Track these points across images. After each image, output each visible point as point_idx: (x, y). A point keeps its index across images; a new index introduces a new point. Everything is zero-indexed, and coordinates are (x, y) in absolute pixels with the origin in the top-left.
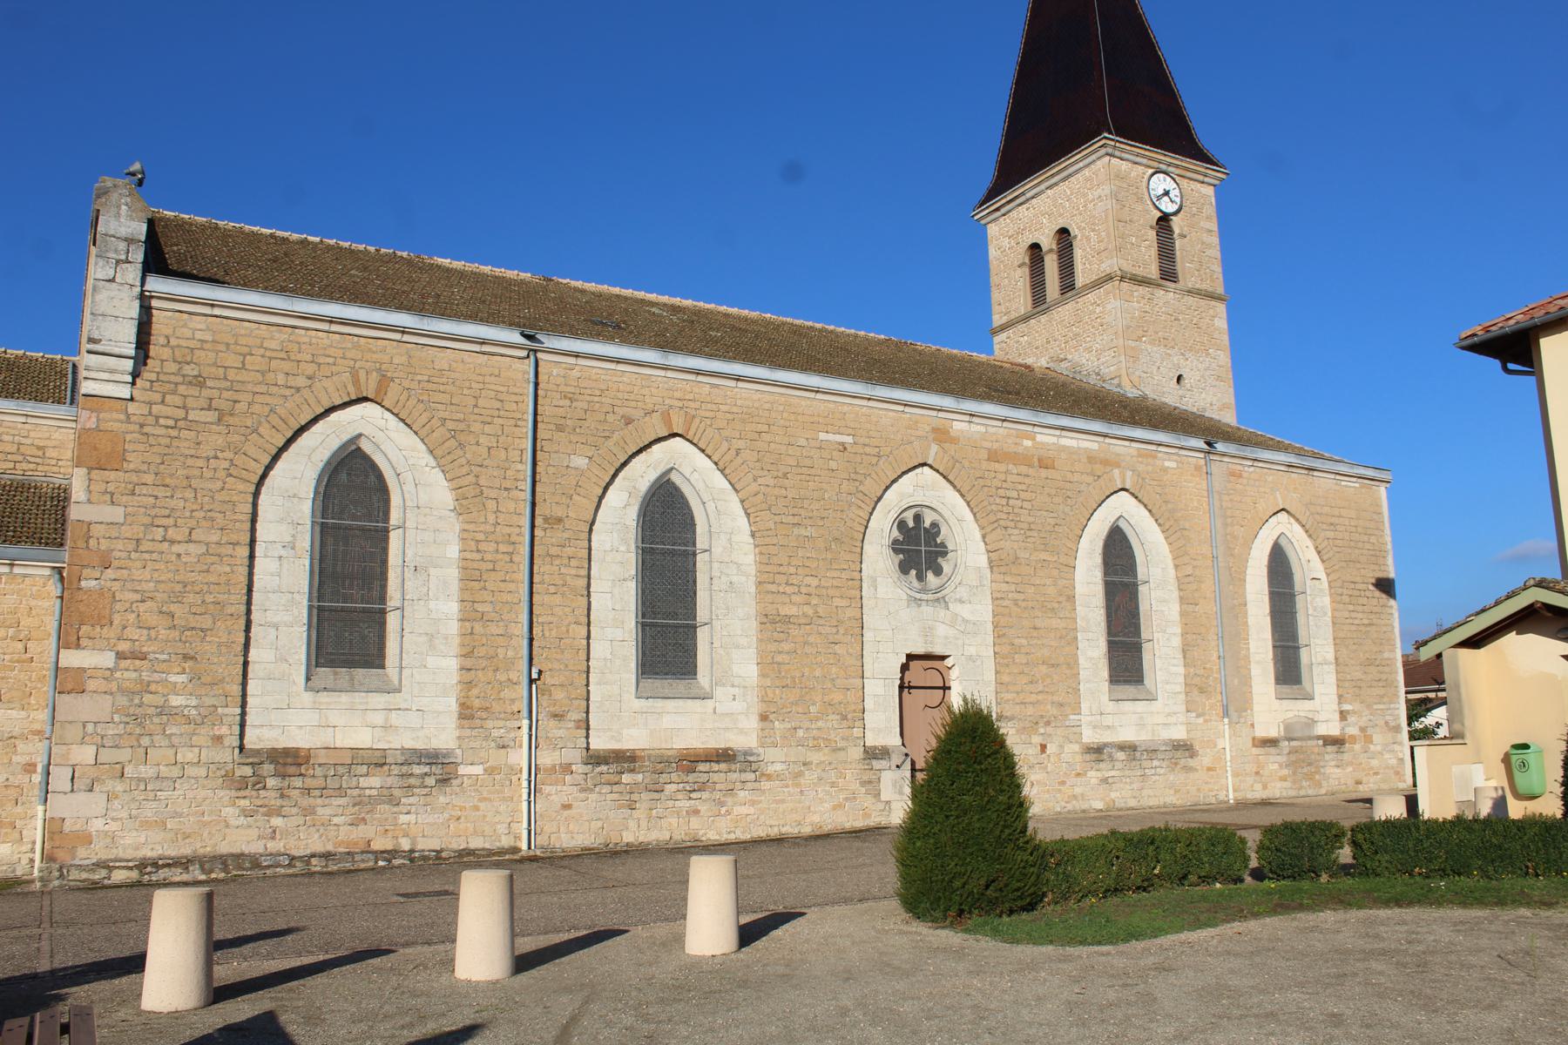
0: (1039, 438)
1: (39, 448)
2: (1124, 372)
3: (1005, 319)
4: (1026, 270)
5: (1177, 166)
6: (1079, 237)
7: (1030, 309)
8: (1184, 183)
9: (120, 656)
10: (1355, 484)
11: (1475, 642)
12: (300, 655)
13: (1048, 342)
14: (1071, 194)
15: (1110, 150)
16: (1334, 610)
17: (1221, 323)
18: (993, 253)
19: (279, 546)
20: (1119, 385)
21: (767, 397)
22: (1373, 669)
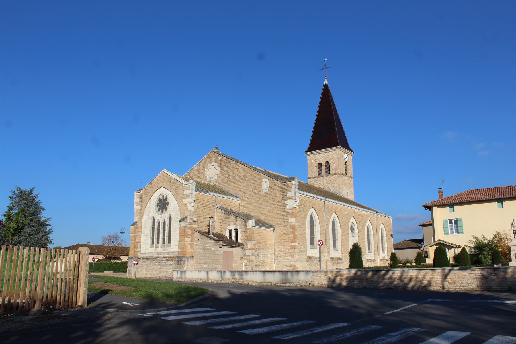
0: (362, 212)
1: (236, 205)
2: (341, 192)
3: (311, 176)
4: (317, 167)
5: (348, 152)
6: (331, 164)
7: (318, 176)
8: (348, 155)
10: (389, 219)
11: (430, 247)
12: (310, 244)
13: (322, 183)
14: (330, 155)
15: (340, 149)
16: (387, 239)
17: (352, 183)
18: (308, 162)
20: (340, 194)
21: (342, 207)
22: (391, 249)
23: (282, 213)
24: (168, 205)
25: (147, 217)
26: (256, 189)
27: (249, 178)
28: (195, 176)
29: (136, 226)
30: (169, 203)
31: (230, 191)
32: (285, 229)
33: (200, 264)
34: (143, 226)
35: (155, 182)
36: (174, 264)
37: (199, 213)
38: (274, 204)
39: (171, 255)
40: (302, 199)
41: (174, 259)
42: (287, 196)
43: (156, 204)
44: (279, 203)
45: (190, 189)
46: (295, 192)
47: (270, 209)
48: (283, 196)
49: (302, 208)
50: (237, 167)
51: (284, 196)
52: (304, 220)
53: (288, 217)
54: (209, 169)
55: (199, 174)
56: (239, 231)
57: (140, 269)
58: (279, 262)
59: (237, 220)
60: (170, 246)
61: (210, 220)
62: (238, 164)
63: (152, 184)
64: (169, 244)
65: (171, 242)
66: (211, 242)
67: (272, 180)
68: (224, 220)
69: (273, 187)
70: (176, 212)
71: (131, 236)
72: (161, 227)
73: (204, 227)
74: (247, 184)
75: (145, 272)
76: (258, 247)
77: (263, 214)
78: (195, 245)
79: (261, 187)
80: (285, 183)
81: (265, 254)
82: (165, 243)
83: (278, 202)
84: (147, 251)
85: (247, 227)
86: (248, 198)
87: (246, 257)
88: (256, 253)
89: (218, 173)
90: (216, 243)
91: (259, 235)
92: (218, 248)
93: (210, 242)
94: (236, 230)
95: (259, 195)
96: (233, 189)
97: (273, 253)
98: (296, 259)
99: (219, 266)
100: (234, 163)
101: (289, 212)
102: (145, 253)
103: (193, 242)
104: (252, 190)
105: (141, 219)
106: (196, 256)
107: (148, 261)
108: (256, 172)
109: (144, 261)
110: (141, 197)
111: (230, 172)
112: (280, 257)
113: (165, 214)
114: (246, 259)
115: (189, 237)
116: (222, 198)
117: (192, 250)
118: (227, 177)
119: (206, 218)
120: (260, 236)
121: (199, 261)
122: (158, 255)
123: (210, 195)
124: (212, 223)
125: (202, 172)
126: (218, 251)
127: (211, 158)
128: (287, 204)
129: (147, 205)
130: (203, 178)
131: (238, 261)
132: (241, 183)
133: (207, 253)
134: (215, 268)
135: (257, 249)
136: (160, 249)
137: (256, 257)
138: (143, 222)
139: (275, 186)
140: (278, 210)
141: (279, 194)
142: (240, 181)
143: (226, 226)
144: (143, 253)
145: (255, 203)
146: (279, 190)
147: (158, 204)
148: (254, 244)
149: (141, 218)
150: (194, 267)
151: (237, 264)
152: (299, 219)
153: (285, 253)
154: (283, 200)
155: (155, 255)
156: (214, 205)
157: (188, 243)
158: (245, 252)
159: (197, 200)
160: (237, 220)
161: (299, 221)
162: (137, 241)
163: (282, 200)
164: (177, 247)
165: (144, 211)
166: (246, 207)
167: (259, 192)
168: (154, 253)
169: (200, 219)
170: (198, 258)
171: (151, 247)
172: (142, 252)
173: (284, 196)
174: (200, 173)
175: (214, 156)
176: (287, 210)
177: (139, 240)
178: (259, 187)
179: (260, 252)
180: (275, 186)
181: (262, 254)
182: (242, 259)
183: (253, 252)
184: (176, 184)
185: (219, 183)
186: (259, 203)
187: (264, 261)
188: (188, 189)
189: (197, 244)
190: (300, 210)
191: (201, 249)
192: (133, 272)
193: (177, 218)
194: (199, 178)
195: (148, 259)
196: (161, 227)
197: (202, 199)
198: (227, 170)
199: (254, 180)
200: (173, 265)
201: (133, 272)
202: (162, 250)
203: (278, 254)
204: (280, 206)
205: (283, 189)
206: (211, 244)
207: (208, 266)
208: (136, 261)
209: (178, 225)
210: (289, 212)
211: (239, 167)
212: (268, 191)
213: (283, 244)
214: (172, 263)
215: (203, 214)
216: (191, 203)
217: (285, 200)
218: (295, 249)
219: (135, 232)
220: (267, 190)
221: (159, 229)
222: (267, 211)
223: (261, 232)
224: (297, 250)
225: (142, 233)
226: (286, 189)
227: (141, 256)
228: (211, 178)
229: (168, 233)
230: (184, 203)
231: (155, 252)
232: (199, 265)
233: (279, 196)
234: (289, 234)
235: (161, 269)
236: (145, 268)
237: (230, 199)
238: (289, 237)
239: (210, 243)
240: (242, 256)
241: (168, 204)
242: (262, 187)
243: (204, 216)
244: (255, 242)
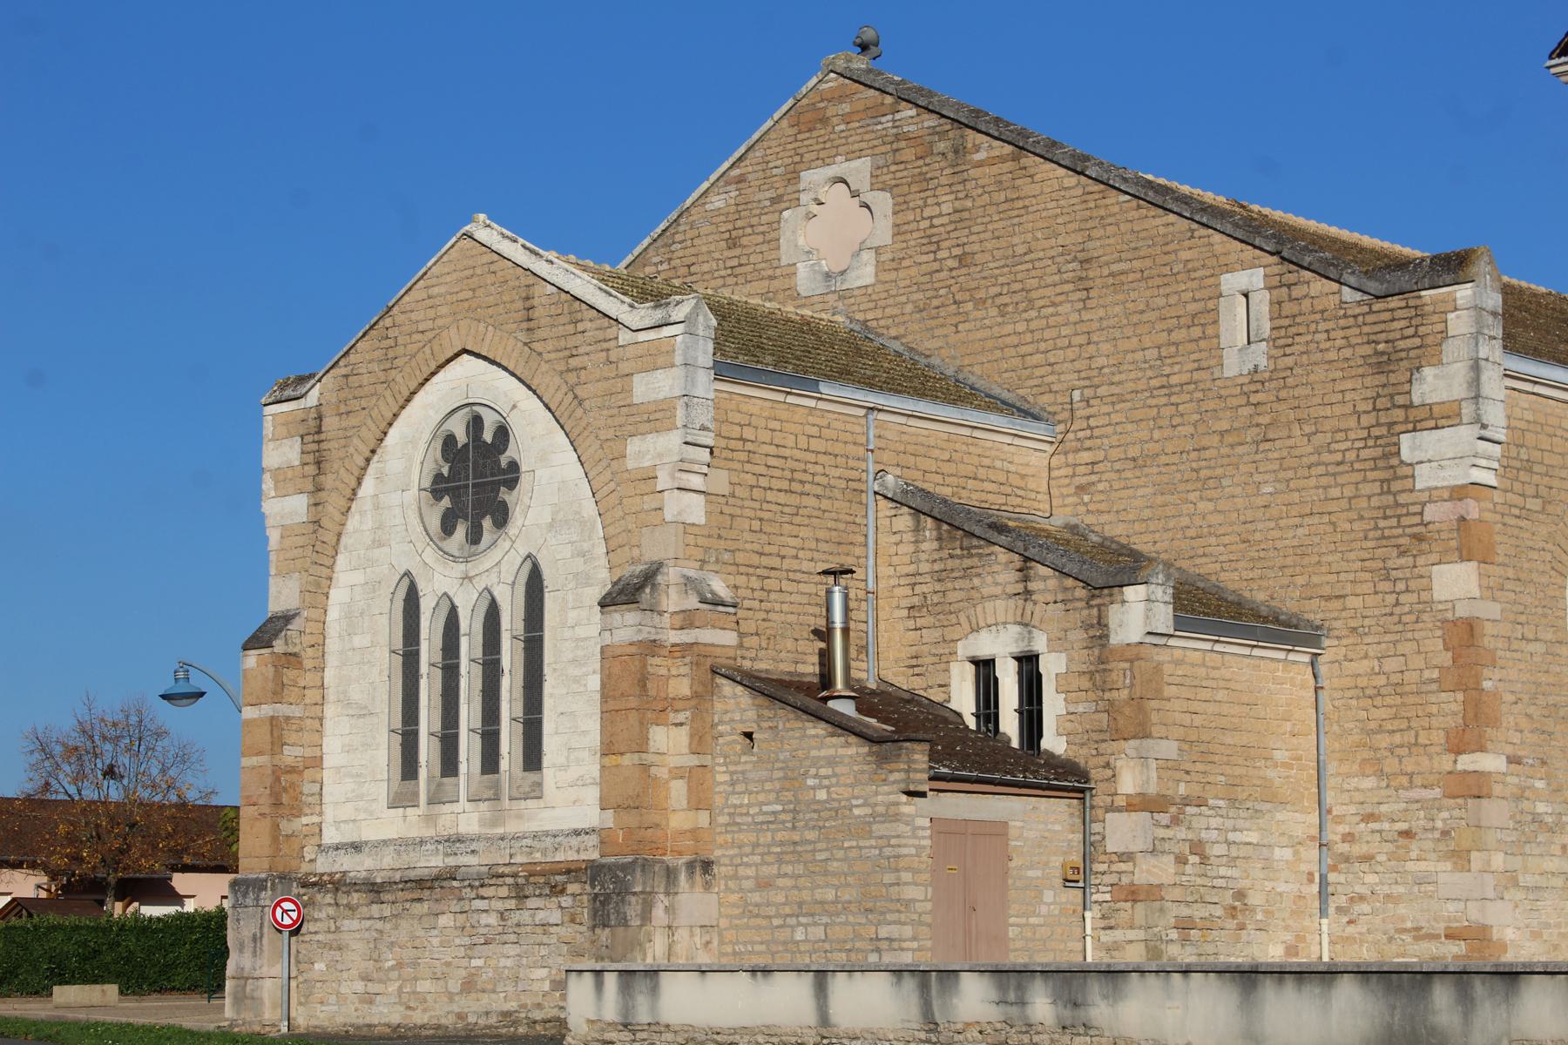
1: (1023, 476)
23: (1376, 528)
24: (512, 483)
25: (358, 577)
26: (1173, 349)
27: (1115, 268)
28: (706, 267)
29: (279, 646)
30: (523, 468)
31: (977, 370)
32: (1401, 648)
33: (764, 922)
34: (332, 645)
35: (413, 316)
36: (573, 921)
37: (747, 536)
38: (1314, 458)
39: (544, 852)
40: (1529, 416)
41: (573, 888)
42: (1416, 400)
43: (427, 483)
44: (1351, 456)
45: (678, 359)
46: (1476, 367)
47: (1280, 499)
48: (1381, 403)
49: (1530, 490)
50: (1028, 188)
51: (1392, 396)
52: (1545, 580)
53: (1421, 561)
54: (815, 208)
55: (737, 252)
56: (1051, 666)
57: (319, 966)
58: (1362, 898)
59: (1032, 586)
60: (536, 792)
61: (829, 592)
62: (1030, 160)
63: (391, 333)
64: (532, 777)
65: (546, 761)
66: (841, 751)
67: (1292, 278)
68: (938, 587)
69: (1302, 329)
70: (575, 539)
71: (248, 723)
72: (470, 647)
73: (790, 644)
74: (1101, 313)
75: (359, 986)
76: (1196, 790)
77: (1226, 540)
78: (721, 778)
79: (1210, 331)
80: (1394, 302)
81: (1253, 837)
82: (504, 764)
83: (1343, 446)
84: (369, 833)
85: (1107, 636)
86: (1115, 418)
87: (1103, 867)
88: (1181, 833)
89: (883, 232)
90: (882, 760)
91: (1205, 694)
92: (892, 798)
93: (831, 752)
94: (1028, 664)
95: (1200, 395)
96: (998, 354)
97: (1315, 832)
98: (1490, 880)
99: (908, 931)
100: (1002, 159)
101: (1427, 518)
102: (356, 847)
103: (707, 760)
104: (1139, 356)
105: (318, 591)
106: (732, 857)
107: (374, 906)
108: (1172, 218)
109: (349, 906)
110: (313, 431)
111: (975, 229)
112: (1365, 867)
113: (496, 555)
114: (1108, 879)
115: (681, 717)
116: (912, 422)
117: (703, 819)
118: (952, 263)
119: (798, 576)
120: (1211, 708)
121: (756, 897)
122: (451, 861)
123: (822, 405)
124: (847, 610)
125: (761, 229)
126: (897, 818)
127: (824, 121)
128: (1418, 456)
129: (361, 493)
130: (771, 278)
131: (1048, 896)
132: (1054, 304)
133: (811, 835)
134: (878, 950)
135: (1186, 802)
136: (465, 817)
137: (1181, 860)
138: (333, 614)
139: (1322, 327)
140: (1344, 504)
141: (1349, 385)
142: (1048, 292)
143: (950, 634)
144: (337, 849)
145: (1164, 459)
146: (1347, 353)
147: (438, 478)
148: (1167, 766)
149: (318, 585)
150: (721, 943)
151: (1042, 921)
152: (1511, 573)
153: (1407, 834)
154: (1384, 430)
155: (434, 861)
156: (854, 474)
157: (673, 761)
158: (1096, 827)
159: (733, 444)
160: (1032, 586)
161: (1509, 585)
162: (290, 754)
163: (1376, 432)
164: (592, 795)
165: (339, 535)
166: (1101, 487)
167: (1196, 376)
168: (422, 842)
169: (755, 583)
170: (750, 872)
171: (399, 801)
172: (330, 836)
173: (1392, 396)
174: (744, 241)
175: (846, 108)
176: (1417, 509)
177: (309, 752)
178: (1196, 332)
179: (1214, 822)
180: (1322, 327)
182: (1077, 878)
183: (1157, 824)
184: (571, 329)
185: (888, 311)
186: (1194, 455)
187: (1240, 895)
188: (661, 361)
189: (740, 768)
190: (1519, 500)
191: (765, 808)
192: (269, 990)
193: (583, 580)
194: (741, 280)
195: (374, 889)
196: (470, 647)
197: (765, 436)
198: (946, 208)
199: (1158, 281)
200: (567, 932)
201: (268, 983)
202: (482, 823)
203: (1349, 838)
204: (1358, 477)
205: (1381, 347)
206: (838, 770)
207: (819, 932)
208: (287, 905)
209: (594, 630)
210: (1427, 518)
211: (1036, 189)
212: (1263, 362)
213: (1391, 765)
214: (555, 917)
215: (774, 549)
216: (686, 466)
217: (1398, 428)
218: (1484, 802)
219: (277, 693)
220: (1260, 355)
221: (457, 666)
222: (1259, 514)
223: (1215, 674)
224: (1495, 812)
225: (331, 695)
226: (1401, 344)
227: (324, 865)
228: (828, 276)
229: (519, 693)
230: (630, 464)
231: (430, 833)
232: (759, 927)
233: (1348, 396)
234: (1434, 687)
235: (476, 963)
236: (356, 957)
237: (977, 434)
238: (1434, 709)
239: (831, 762)
240: (1076, 858)
241: (512, 476)
242: (1218, 336)
243: (786, 564)
244: (1168, 749)
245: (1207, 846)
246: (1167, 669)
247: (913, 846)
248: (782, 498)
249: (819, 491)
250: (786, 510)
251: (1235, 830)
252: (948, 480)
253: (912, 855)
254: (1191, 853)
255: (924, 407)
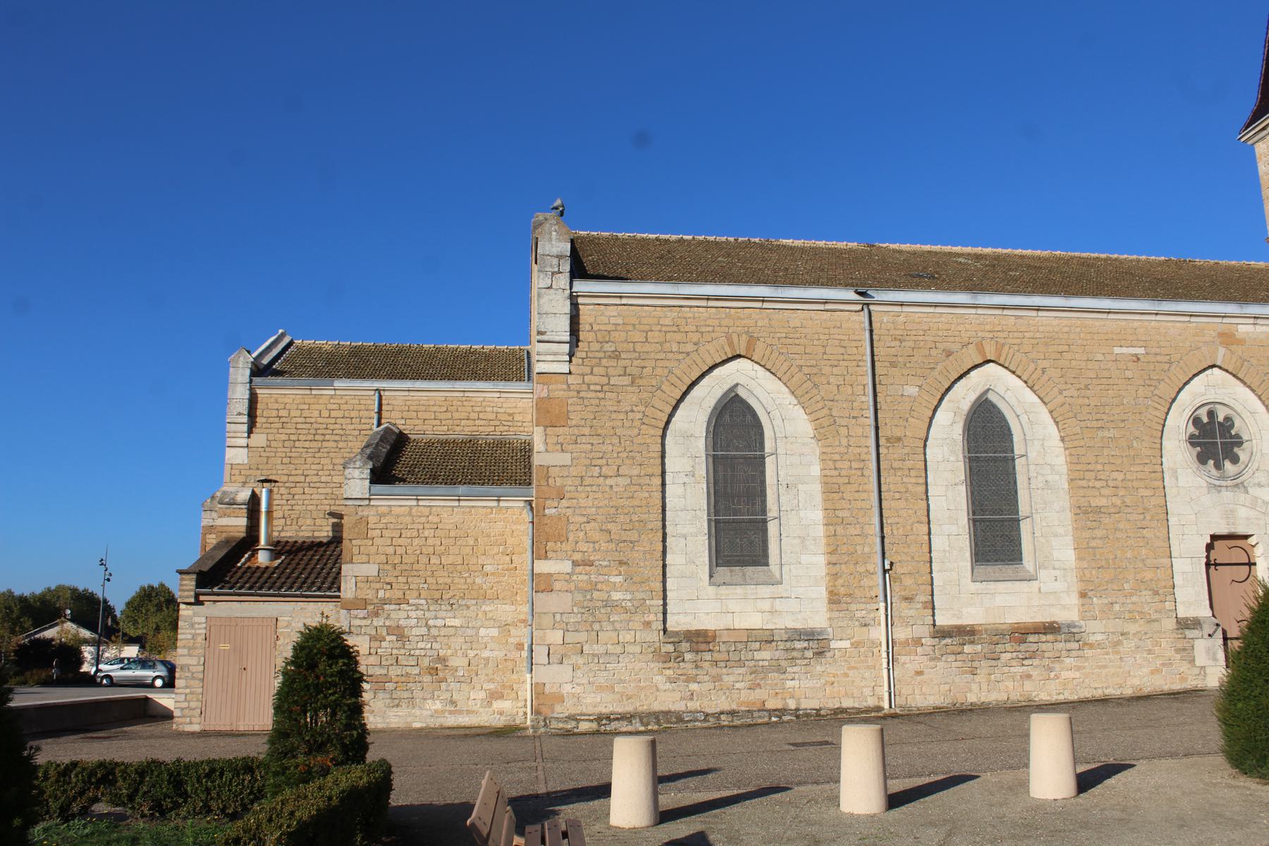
1: (510, 415)
9: (575, 564)
12: (704, 557)
19: (683, 475)
21: (1065, 322)
37: (279, 467)
81: (457, 622)
88: (378, 622)
116: (412, 393)
123: (338, 392)
135: (385, 602)
179: (413, 614)
181: (429, 628)
237: (466, 394)
245: (406, 630)
246: (372, 520)
247: (190, 633)
248: (307, 444)
249: (337, 438)
250: (309, 450)
251: (436, 618)
252: (444, 423)
253: (188, 639)
254: (388, 634)
255: (419, 384)
